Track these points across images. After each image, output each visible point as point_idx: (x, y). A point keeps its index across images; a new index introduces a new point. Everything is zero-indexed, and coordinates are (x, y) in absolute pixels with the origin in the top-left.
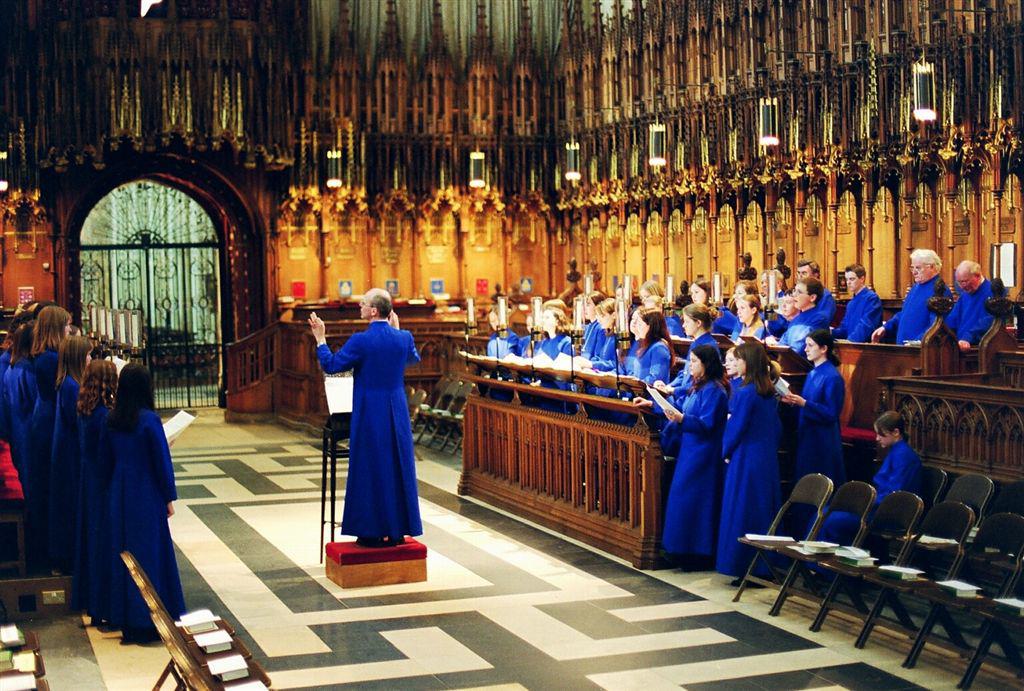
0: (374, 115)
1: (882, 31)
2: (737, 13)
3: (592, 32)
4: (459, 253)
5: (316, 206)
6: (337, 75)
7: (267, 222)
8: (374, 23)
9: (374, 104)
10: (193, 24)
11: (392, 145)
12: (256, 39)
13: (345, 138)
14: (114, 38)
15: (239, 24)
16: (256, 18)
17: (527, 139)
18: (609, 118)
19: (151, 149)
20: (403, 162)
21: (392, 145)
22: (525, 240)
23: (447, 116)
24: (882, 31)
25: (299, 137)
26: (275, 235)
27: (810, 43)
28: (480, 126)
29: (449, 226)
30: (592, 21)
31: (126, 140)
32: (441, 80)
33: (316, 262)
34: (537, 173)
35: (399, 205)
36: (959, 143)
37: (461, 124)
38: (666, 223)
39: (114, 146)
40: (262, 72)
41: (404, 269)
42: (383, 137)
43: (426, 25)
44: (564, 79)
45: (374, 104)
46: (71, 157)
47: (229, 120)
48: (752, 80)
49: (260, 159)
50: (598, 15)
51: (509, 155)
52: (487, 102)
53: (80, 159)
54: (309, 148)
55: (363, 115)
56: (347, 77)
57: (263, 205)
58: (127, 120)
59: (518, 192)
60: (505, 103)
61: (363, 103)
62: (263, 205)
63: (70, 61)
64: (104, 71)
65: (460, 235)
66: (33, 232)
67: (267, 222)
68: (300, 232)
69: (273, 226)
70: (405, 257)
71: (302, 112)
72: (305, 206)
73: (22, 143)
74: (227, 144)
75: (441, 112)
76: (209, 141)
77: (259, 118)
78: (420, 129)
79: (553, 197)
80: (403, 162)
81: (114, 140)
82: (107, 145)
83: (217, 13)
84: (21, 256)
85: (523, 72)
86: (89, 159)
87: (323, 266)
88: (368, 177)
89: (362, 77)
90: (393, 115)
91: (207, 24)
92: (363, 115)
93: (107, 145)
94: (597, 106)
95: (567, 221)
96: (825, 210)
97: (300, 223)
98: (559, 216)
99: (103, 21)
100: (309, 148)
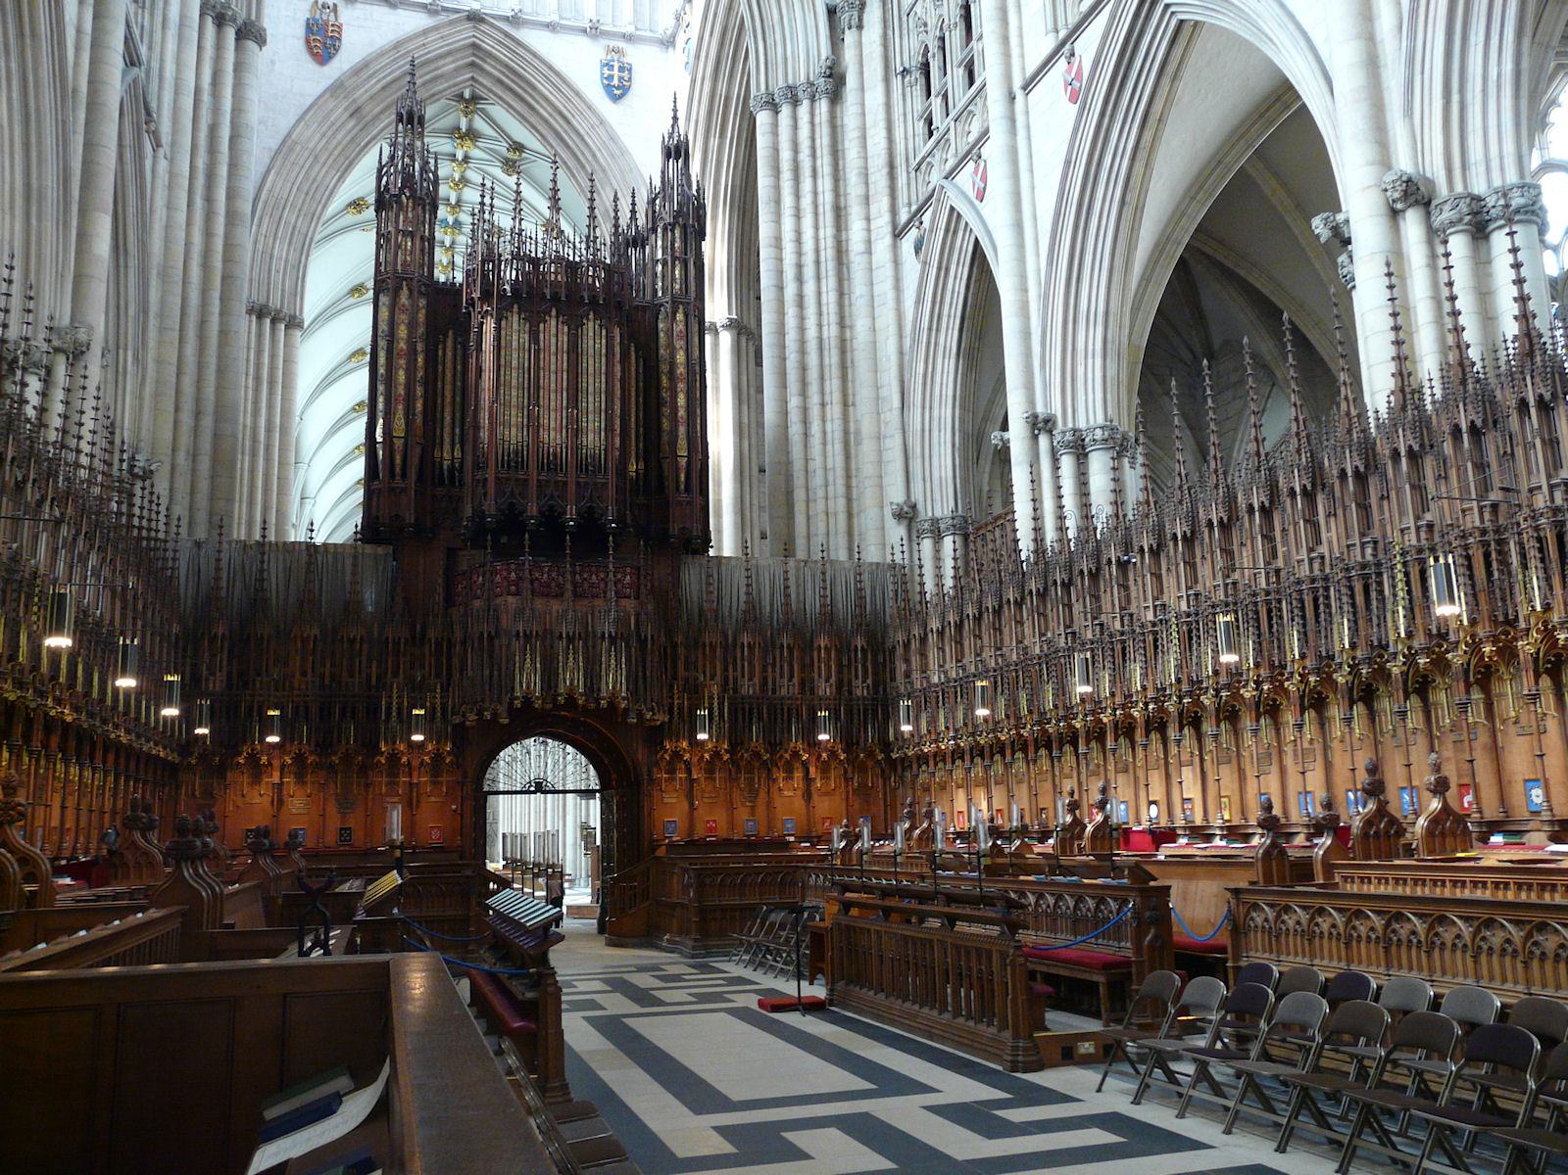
0: (735, 680)
1: (1179, 589)
2: (1046, 583)
3: (918, 607)
4: (808, 796)
5: (687, 756)
6: (704, 645)
7: (645, 770)
8: (735, 604)
9: (735, 670)
10: (585, 602)
11: (751, 704)
12: (637, 615)
13: (711, 698)
14: (520, 611)
15: (624, 602)
16: (637, 598)
17: (864, 698)
18: (935, 679)
19: (549, 706)
20: (760, 719)
21: (751, 704)
22: (863, 785)
23: (796, 680)
24: (1179, 589)
25: (672, 698)
26: (651, 780)
27: (1113, 605)
28: (825, 689)
29: (798, 775)
30: (918, 598)
31: (527, 700)
32: (790, 650)
33: (686, 805)
34: (873, 728)
35: (757, 755)
36: (1258, 683)
37: (808, 686)
38: (987, 769)
39: (517, 704)
40: (643, 642)
41: (761, 810)
42: (743, 698)
43: (779, 599)
44: (894, 647)
45: (735, 670)
46: (480, 713)
47: (614, 680)
48: (1063, 640)
49: (640, 715)
50: (923, 593)
51: (849, 712)
52: (830, 667)
53: (488, 715)
54: (681, 708)
55: (726, 679)
56: (713, 648)
57: (641, 755)
58: (528, 680)
59: (858, 743)
60: (845, 670)
61: (726, 670)
62: (641, 755)
63: (482, 634)
64: (510, 640)
65: (808, 781)
66: (444, 779)
67: (645, 770)
68: (673, 779)
69: (650, 773)
70: (762, 795)
71: (675, 677)
72: (677, 755)
73: (438, 701)
74: (612, 705)
75: (791, 677)
76: (598, 700)
77: (641, 681)
78: (774, 691)
79: (887, 747)
80: (760, 719)
81: (517, 698)
82: (511, 704)
83: (605, 592)
84: (433, 799)
85: (859, 642)
86: (495, 714)
87: (692, 808)
88: (730, 733)
89: (725, 648)
90: (750, 679)
91: (597, 602)
92: (726, 679)
93: (511, 704)
94: (924, 669)
95: (899, 768)
96: (1133, 749)
97: (671, 771)
98: (892, 763)
99: (510, 599)
100: (681, 708)
